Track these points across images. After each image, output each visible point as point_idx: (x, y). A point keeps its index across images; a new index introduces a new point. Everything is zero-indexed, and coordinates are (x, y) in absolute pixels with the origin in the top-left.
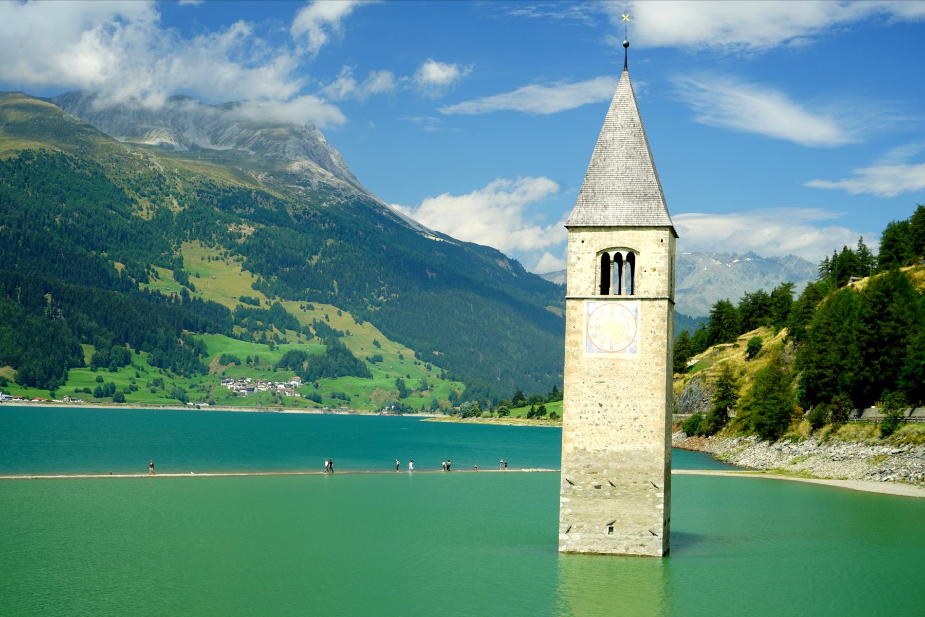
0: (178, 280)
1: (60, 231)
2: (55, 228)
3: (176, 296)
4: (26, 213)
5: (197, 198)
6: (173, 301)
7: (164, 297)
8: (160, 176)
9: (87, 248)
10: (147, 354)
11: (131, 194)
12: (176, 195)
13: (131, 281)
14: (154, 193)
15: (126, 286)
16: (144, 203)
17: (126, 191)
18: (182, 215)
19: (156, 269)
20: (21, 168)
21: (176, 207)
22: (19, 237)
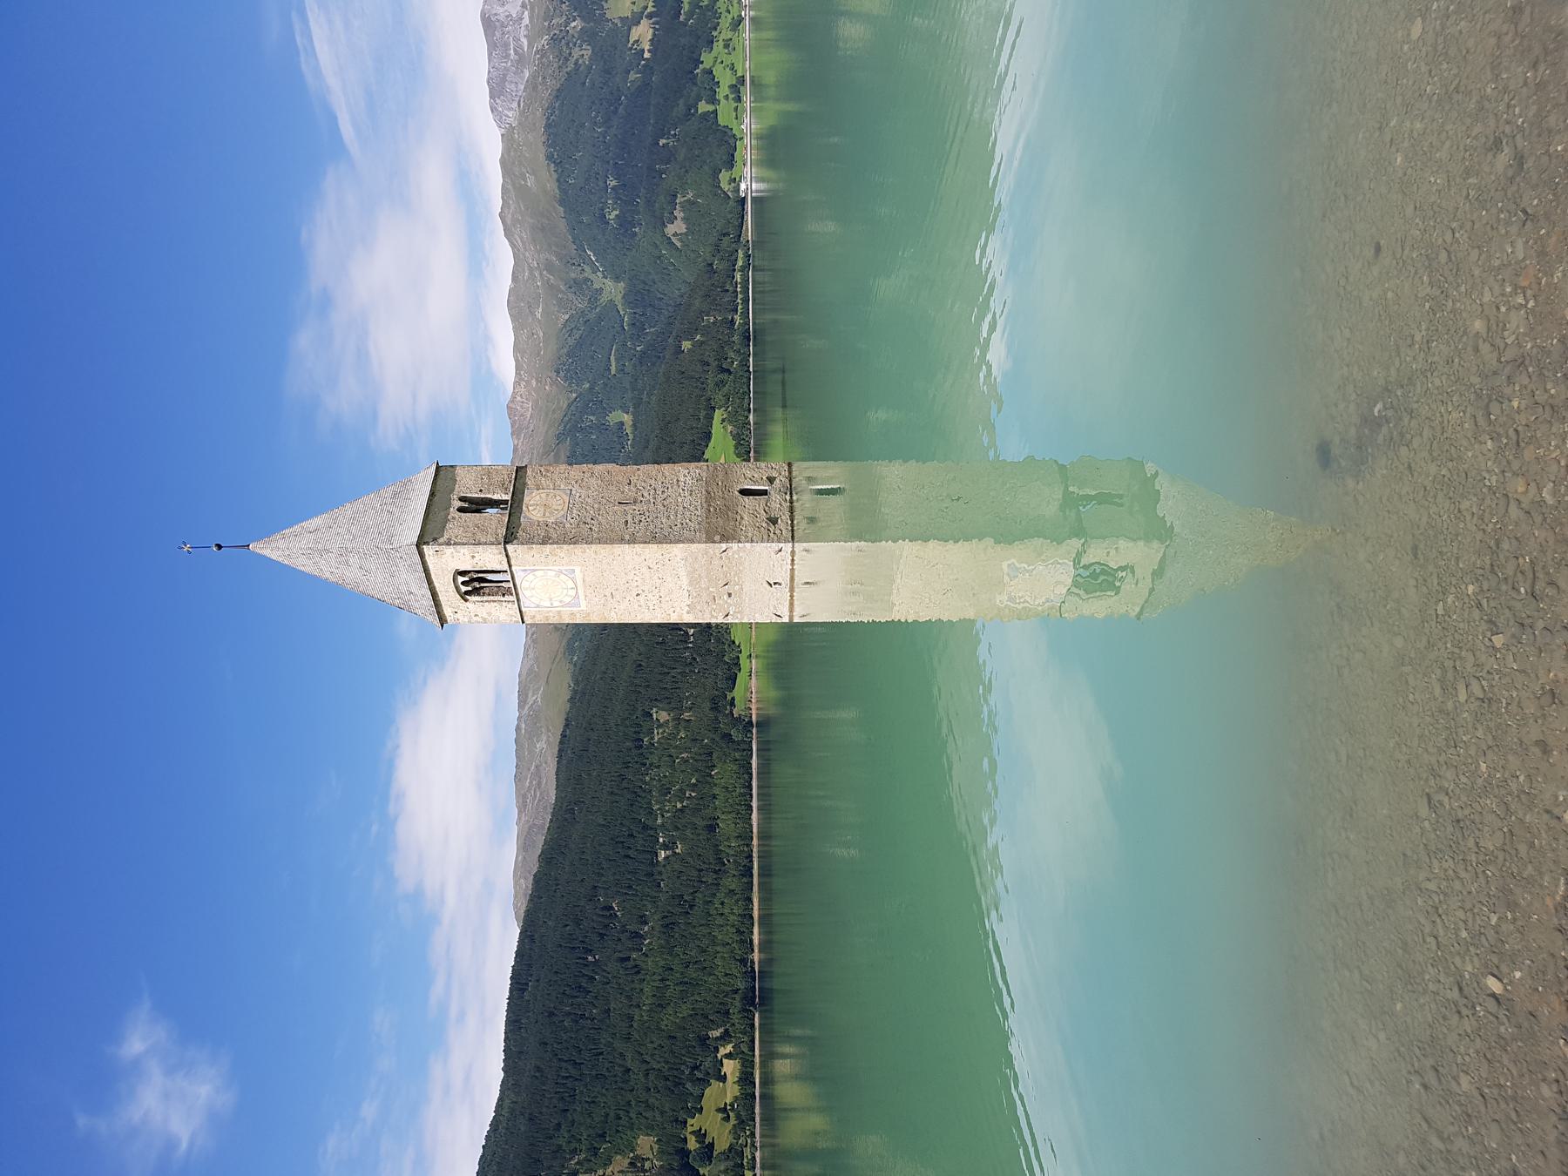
0: (639, 23)
1: (609, 128)
2: (606, 132)
3: (653, 24)
4: (597, 157)
5: (567, 4)
6: (657, 27)
7: (654, 35)
8: (552, 39)
9: (620, 105)
10: (703, 54)
11: (571, 66)
12: (567, 24)
13: (643, 66)
14: (568, 44)
15: (648, 69)
16: (576, 53)
17: (569, 69)
18: (583, 18)
19: (631, 42)
20: (561, 162)
21: (576, 24)
22: (616, 163)
